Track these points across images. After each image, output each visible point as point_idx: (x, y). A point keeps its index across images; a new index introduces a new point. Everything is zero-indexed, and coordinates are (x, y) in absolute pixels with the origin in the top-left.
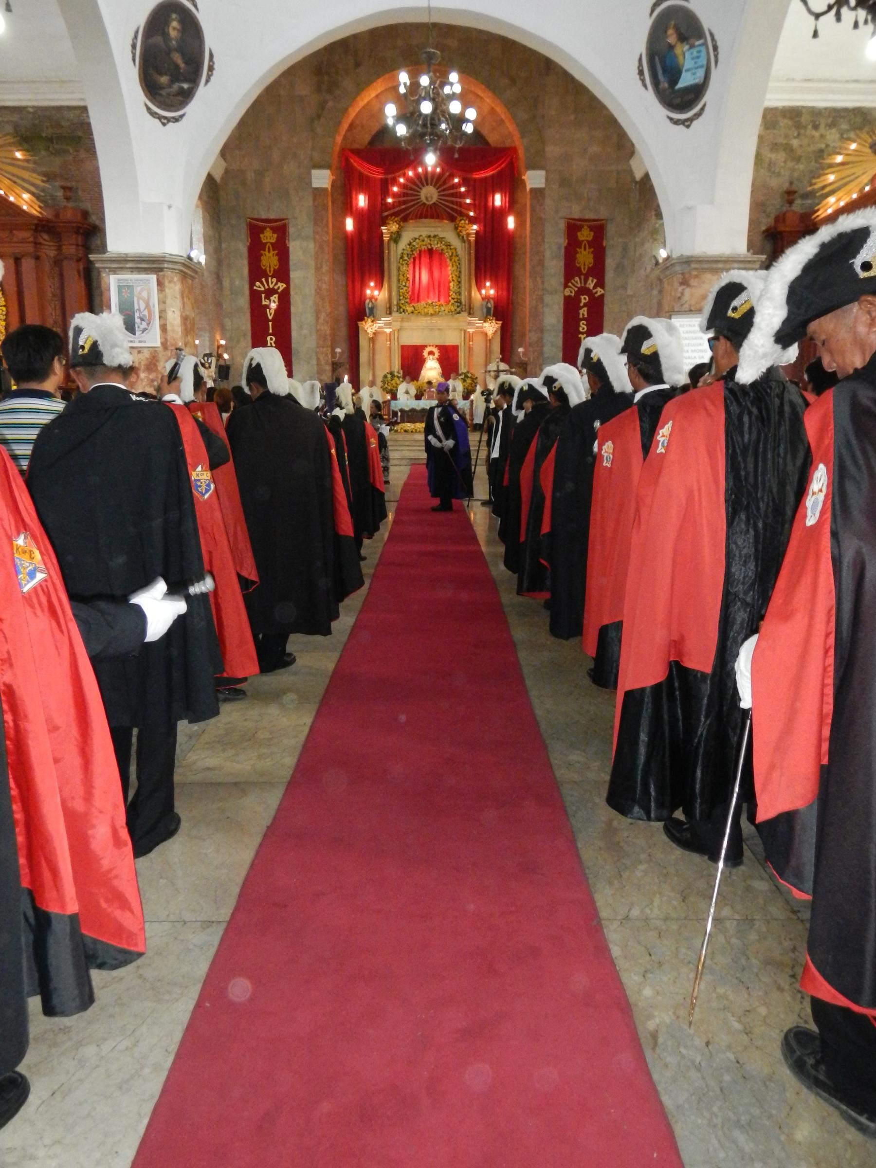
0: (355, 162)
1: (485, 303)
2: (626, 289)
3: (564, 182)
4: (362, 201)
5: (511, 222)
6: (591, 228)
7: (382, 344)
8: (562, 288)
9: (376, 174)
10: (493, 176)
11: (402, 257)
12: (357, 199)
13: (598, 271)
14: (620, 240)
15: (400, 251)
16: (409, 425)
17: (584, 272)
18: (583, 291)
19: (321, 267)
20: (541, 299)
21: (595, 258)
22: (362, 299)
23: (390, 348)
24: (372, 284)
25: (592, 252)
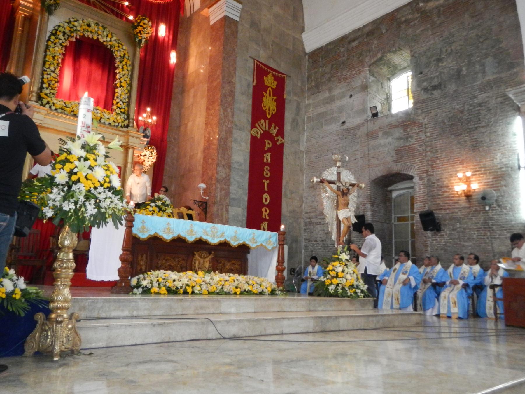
1: (141, 129)
2: (299, 144)
3: (254, 25)
5: (173, 58)
6: (276, 78)
8: (249, 128)
11: (54, 33)
13: (278, 119)
14: (295, 98)
15: (50, 27)
16: (173, 275)
17: (269, 117)
18: (266, 135)
20: (230, 132)
21: (277, 106)
25: (275, 101)
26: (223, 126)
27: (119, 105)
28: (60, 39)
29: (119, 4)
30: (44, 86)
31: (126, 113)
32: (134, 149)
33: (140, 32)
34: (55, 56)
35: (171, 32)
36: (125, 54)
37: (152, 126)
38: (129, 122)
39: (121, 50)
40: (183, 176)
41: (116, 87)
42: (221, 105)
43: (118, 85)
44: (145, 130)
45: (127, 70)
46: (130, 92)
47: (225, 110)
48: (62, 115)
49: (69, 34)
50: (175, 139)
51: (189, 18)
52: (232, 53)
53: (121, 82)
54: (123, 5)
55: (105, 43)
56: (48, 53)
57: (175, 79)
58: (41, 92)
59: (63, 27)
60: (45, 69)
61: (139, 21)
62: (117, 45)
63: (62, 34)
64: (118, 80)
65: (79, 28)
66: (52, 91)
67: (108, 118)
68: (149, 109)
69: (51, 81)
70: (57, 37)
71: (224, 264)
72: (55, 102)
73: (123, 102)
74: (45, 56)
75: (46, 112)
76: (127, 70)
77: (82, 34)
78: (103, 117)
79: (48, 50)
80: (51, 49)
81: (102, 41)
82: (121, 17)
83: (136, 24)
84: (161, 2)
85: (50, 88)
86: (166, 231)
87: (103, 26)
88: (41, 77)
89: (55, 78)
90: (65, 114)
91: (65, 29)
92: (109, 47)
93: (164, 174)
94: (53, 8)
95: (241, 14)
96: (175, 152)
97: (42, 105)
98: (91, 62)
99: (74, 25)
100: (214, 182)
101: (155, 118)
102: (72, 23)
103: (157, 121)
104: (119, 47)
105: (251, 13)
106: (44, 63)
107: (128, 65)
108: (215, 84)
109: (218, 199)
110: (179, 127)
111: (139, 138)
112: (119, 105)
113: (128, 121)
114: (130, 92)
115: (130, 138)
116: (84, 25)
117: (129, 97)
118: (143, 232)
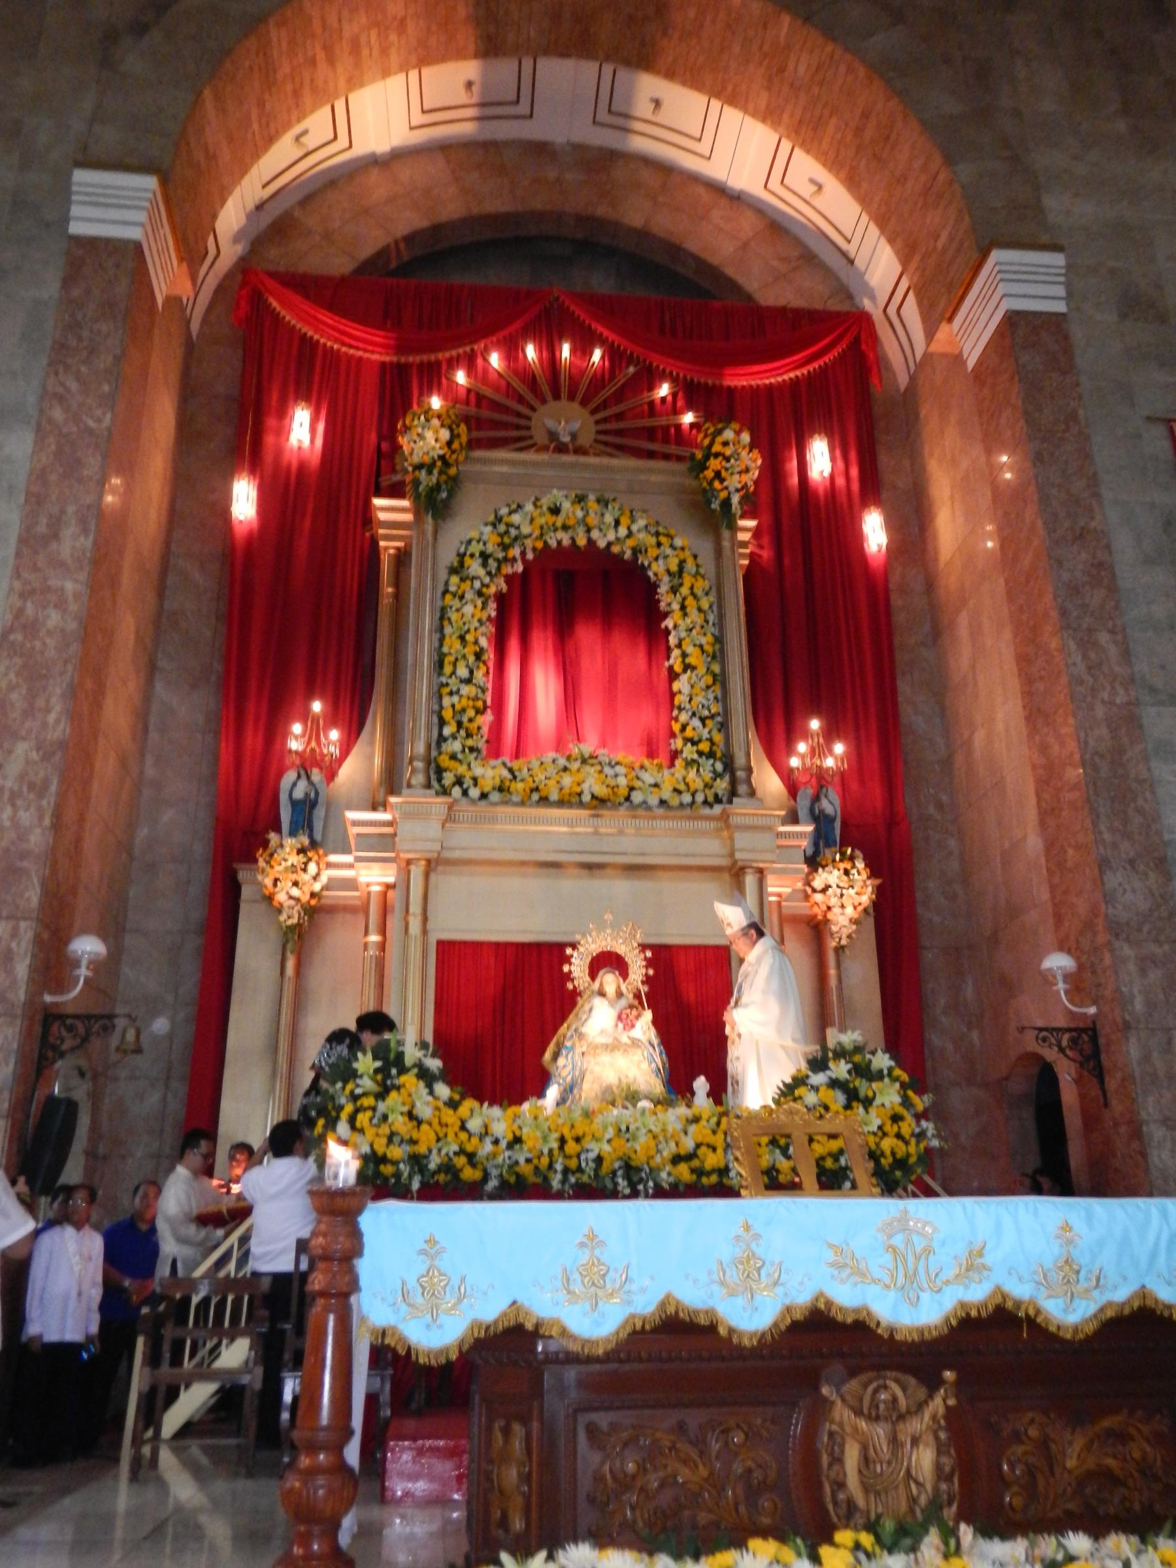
0: (290, 313)
1: (803, 803)
3: (1137, 305)
4: (302, 430)
5: (874, 532)
7: (345, 950)
9: (369, 349)
10: (795, 383)
11: (458, 569)
12: (283, 431)
15: (448, 557)
19: (55, 536)
20: (1128, 721)
22: (271, 756)
23: (380, 964)
24: (317, 706)
26: (1091, 708)
27: (689, 733)
28: (473, 578)
29: (668, 427)
30: (447, 731)
31: (719, 754)
32: (761, 872)
33: (718, 475)
34: (468, 631)
35: (853, 455)
36: (682, 563)
37: (843, 776)
38: (733, 783)
39: (669, 551)
40: (994, 940)
41: (673, 676)
42: (1068, 627)
43: (678, 668)
44: (816, 798)
45: (700, 610)
46: (720, 680)
47: (1087, 643)
48: (501, 809)
49: (501, 555)
50: (940, 806)
51: (906, 390)
52: (1067, 429)
53: (684, 655)
54: (678, 427)
55: (616, 549)
56: (448, 630)
57: (896, 600)
58: (440, 753)
59: (478, 541)
60: (444, 680)
61: (707, 442)
62: (653, 540)
63: (480, 561)
64: (676, 653)
65: (526, 530)
66: (470, 742)
67: (656, 785)
68: (815, 724)
69: (464, 710)
70: (465, 573)
71: (1044, 1444)
72: (478, 771)
73: (703, 720)
74: (441, 645)
75: (444, 810)
76: (700, 610)
77: (540, 545)
78: (637, 784)
79: (446, 623)
80: (454, 616)
81: (602, 544)
82: (679, 459)
83: (699, 455)
84: (798, 373)
85: (463, 733)
86: (577, 1288)
87: (598, 501)
88: (436, 707)
89: (476, 698)
90: (516, 804)
91: (485, 544)
92: (628, 555)
93: (925, 942)
94: (444, 495)
95: (1068, 285)
96: (950, 853)
97: (445, 792)
98: (607, 626)
99: (508, 525)
100: (1102, 938)
101: (839, 748)
102: (505, 519)
103: (847, 754)
104: (659, 544)
105: (1112, 272)
106: (440, 665)
107: (699, 592)
108: (1027, 560)
109: (1139, 1005)
110: (947, 763)
111: (770, 829)
112: (689, 733)
113: (727, 778)
114: (720, 680)
115: (737, 835)
116: (542, 515)
117: (724, 698)
118: (434, 1310)
